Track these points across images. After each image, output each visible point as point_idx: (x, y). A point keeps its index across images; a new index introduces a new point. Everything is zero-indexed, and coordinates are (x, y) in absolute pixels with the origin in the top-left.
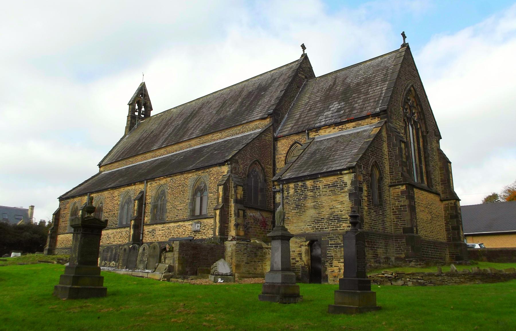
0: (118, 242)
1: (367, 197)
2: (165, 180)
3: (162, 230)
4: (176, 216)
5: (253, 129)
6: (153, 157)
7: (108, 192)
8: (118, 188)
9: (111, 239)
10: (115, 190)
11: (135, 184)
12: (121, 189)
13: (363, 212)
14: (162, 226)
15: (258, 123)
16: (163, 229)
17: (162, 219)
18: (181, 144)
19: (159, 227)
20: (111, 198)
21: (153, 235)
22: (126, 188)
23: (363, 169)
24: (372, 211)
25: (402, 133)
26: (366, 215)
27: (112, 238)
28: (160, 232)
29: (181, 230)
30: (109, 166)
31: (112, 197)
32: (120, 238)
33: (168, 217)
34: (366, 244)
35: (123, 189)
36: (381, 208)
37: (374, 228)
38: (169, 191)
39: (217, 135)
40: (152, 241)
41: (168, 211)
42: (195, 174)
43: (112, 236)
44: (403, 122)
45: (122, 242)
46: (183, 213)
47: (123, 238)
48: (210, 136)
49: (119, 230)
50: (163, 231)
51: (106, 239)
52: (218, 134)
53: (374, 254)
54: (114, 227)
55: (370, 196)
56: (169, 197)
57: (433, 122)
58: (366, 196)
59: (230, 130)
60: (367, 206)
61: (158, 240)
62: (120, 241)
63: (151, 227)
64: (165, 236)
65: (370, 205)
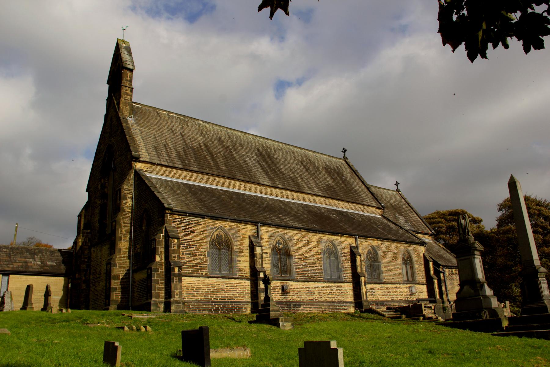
0: (327, 298)
2: (376, 242)
3: (381, 290)
4: (392, 278)
5: (369, 212)
6: (261, 193)
7: (298, 232)
8: (316, 233)
9: (315, 295)
10: (310, 234)
11: (342, 235)
12: (320, 235)
14: (380, 285)
15: (374, 209)
16: (382, 289)
17: (380, 279)
18: (304, 195)
19: (377, 286)
20: (305, 242)
21: (373, 294)
22: (327, 236)
27: (317, 294)
28: (380, 292)
29: (398, 292)
30: (164, 168)
31: (305, 241)
32: (330, 294)
33: (385, 278)
35: (323, 235)
38: (382, 254)
39: (342, 203)
40: (372, 299)
41: (384, 272)
42: (403, 245)
43: (316, 291)
45: (334, 299)
46: (398, 277)
47: (334, 294)
48: (336, 201)
49: (325, 284)
50: (382, 291)
51: (306, 294)
52: (343, 203)
54: (316, 279)
56: (382, 259)
59: (354, 205)
61: (378, 299)
62: (331, 298)
63: (369, 286)
64: (385, 296)
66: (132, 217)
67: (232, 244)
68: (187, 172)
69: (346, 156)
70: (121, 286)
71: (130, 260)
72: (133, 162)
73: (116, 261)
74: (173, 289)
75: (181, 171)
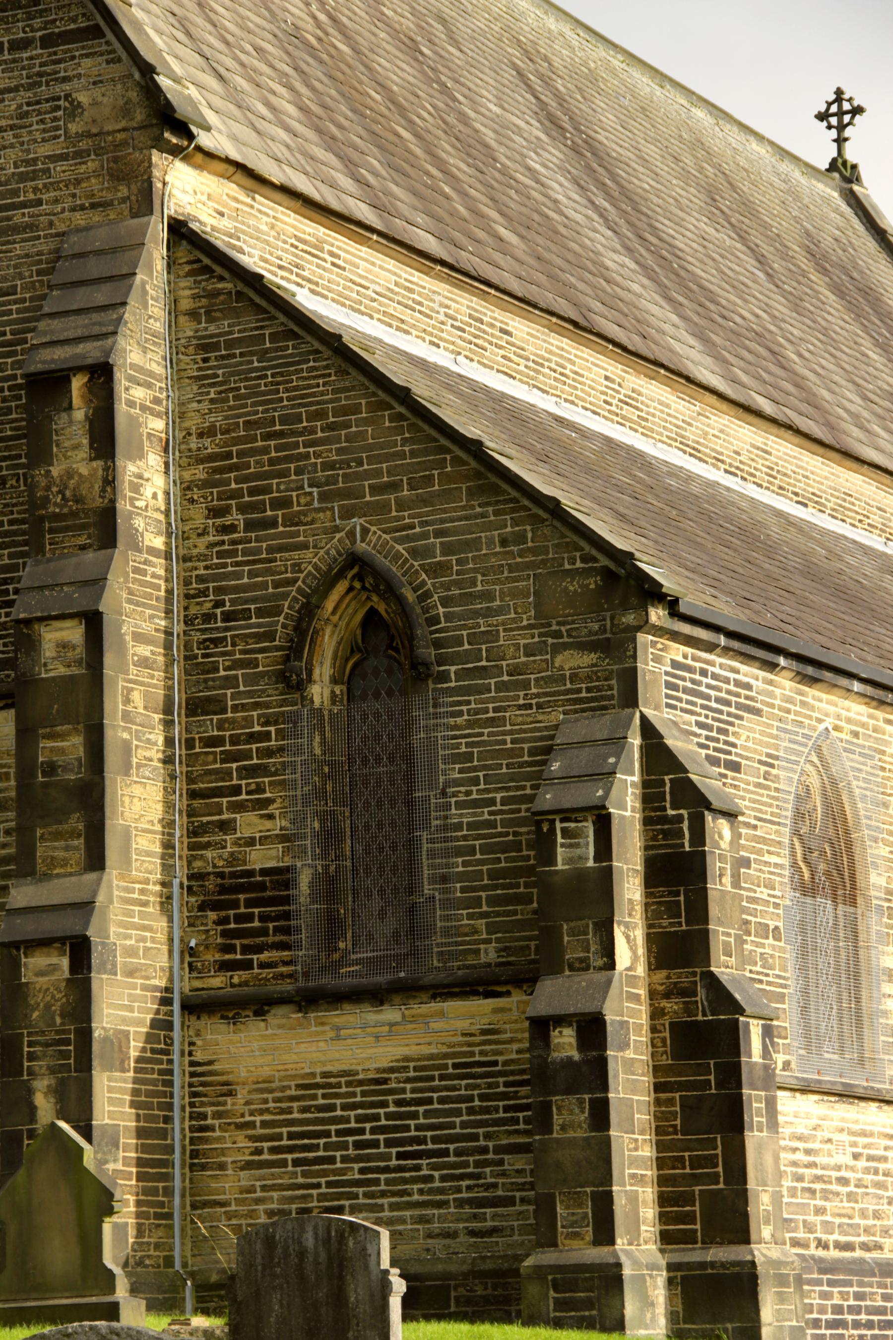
66: (170, 592)
67: (857, 850)
68: (391, 264)
69: (851, 154)
70: (138, 1118)
71: (170, 920)
72: (156, 157)
73: (112, 929)
74: (751, 1185)
75: (364, 251)
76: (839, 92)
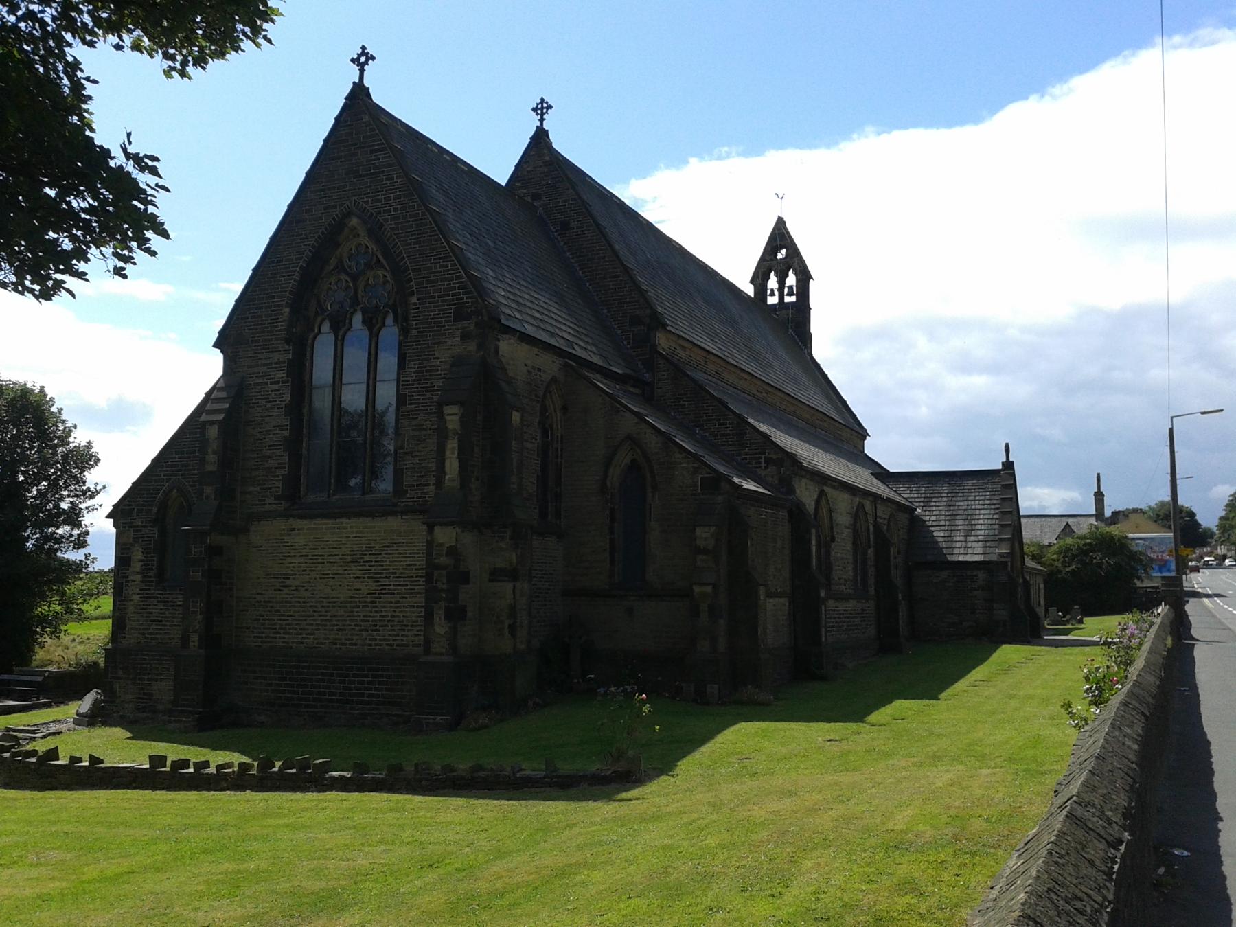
1: (143, 573)
13: (125, 608)
23: (137, 515)
24: (154, 601)
25: (277, 383)
26: (135, 613)
34: (120, 673)
36: (180, 590)
37: (152, 639)
44: (287, 347)
53: (140, 694)
55: (152, 569)
57: (459, 277)
58: (138, 573)
60: (139, 594)
65: (149, 590)
76: (542, 100)
